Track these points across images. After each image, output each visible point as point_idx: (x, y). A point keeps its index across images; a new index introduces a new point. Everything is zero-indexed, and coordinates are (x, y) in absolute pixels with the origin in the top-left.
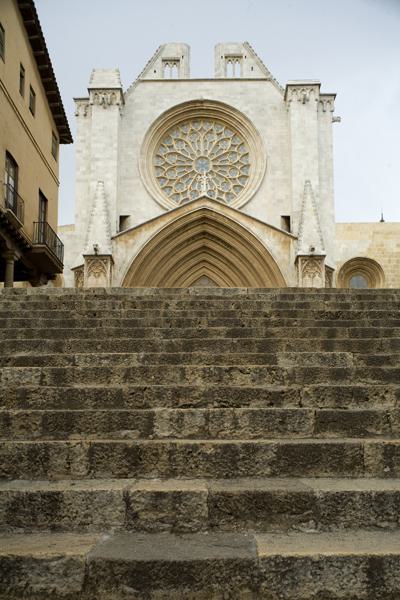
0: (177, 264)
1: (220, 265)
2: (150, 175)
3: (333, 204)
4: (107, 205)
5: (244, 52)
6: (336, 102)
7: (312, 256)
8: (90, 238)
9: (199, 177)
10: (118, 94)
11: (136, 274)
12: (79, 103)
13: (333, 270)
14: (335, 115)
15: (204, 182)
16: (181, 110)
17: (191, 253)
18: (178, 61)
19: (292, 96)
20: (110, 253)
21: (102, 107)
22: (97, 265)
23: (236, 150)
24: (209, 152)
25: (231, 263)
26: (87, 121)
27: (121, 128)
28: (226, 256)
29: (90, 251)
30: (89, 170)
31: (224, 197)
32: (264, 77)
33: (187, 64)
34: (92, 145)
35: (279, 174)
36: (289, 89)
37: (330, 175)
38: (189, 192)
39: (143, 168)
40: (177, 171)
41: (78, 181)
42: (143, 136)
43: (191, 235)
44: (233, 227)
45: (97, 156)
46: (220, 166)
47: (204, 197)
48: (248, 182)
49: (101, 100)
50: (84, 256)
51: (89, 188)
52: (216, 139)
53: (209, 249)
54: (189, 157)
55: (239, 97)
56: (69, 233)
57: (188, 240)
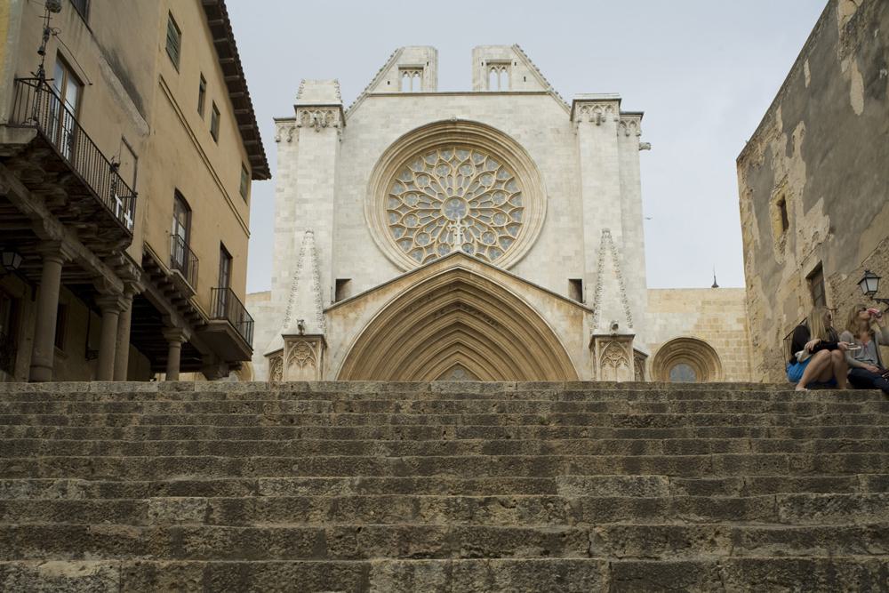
0: (418, 347)
1: (481, 349)
2: (380, 224)
3: (643, 263)
4: (318, 263)
5: (513, 57)
6: (644, 124)
7: (614, 336)
8: (292, 310)
9: (450, 225)
10: (337, 113)
11: (359, 363)
12: (281, 124)
13: (646, 356)
14: (643, 140)
15: (458, 232)
16: (425, 134)
17: (440, 332)
18: (422, 69)
19: (583, 115)
20: (320, 332)
21: (313, 129)
22: (303, 349)
23: (503, 188)
24: (465, 190)
25: (496, 346)
26: (292, 148)
27: (339, 157)
28: (486, 334)
29: (292, 329)
30: (293, 216)
31: (486, 253)
32: (543, 90)
33: (434, 73)
34: (299, 181)
35: (565, 221)
36: (577, 106)
37: (639, 222)
38: (436, 246)
39: (370, 212)
40: (420, 217)
41: (278, 230)
42: (371, 169)
43: (441, 305)
44: (500, 295)
45: (306, 196)
46: (481, 210)
47: (458, 253)
48: (521, 233)
49: (312, 121)
50: (284, 336)
51: (293, 240)
53: (466, 326)
55: (507, 116)
56: (263, 303)
57: (435, 314)
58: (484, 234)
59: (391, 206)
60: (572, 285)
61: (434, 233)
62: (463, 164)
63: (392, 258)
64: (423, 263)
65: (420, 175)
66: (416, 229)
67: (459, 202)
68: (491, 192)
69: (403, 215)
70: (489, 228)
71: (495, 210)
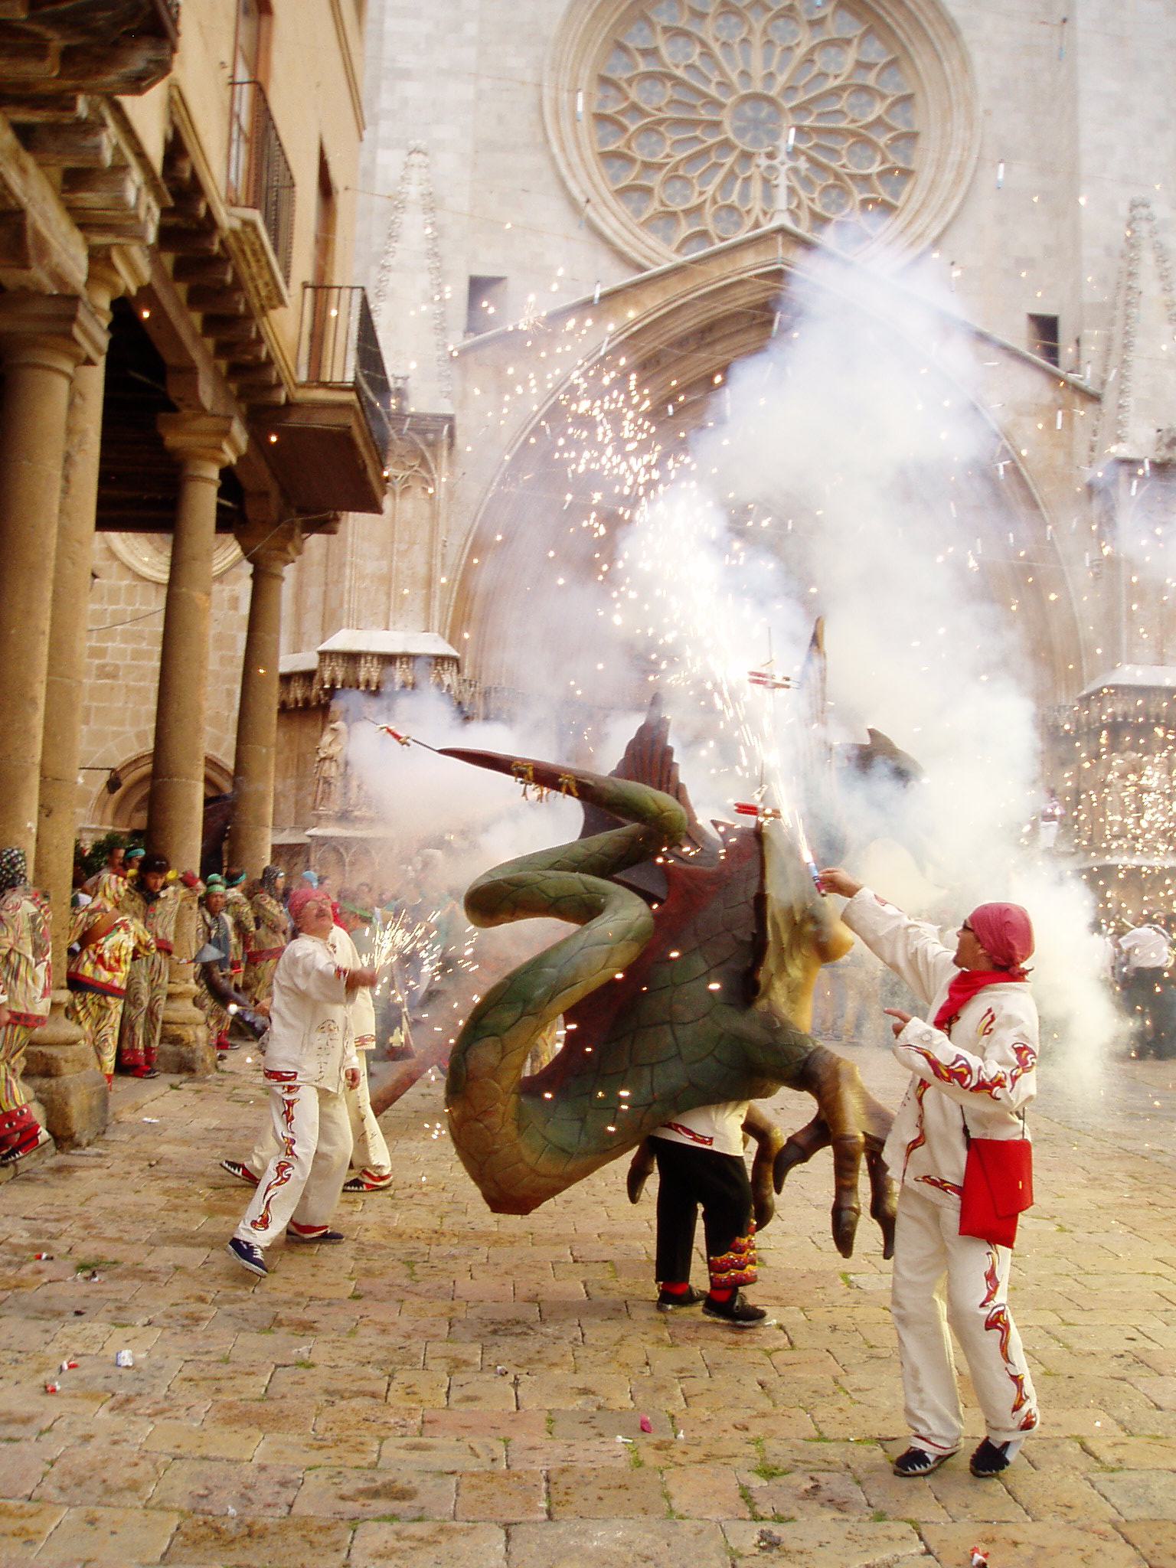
23: (870, 79)
24: (782, 79)
38: (709, 210)
40: (672, 136)
47: (782, 230)
52: (805, 40)
54: (712, 91)
58: (826, 190)
59: (602, 104)
60: (1033, 327)
61: (704, 178)
62: (777, 16)
63: (608, 232)
64: (678, 250)
65: (675, 33)
66: (661, 166)
67: (765, 111)
68: (842, 88)
69: (632, 128)
70: (837, 176)
71: (852, 133)
